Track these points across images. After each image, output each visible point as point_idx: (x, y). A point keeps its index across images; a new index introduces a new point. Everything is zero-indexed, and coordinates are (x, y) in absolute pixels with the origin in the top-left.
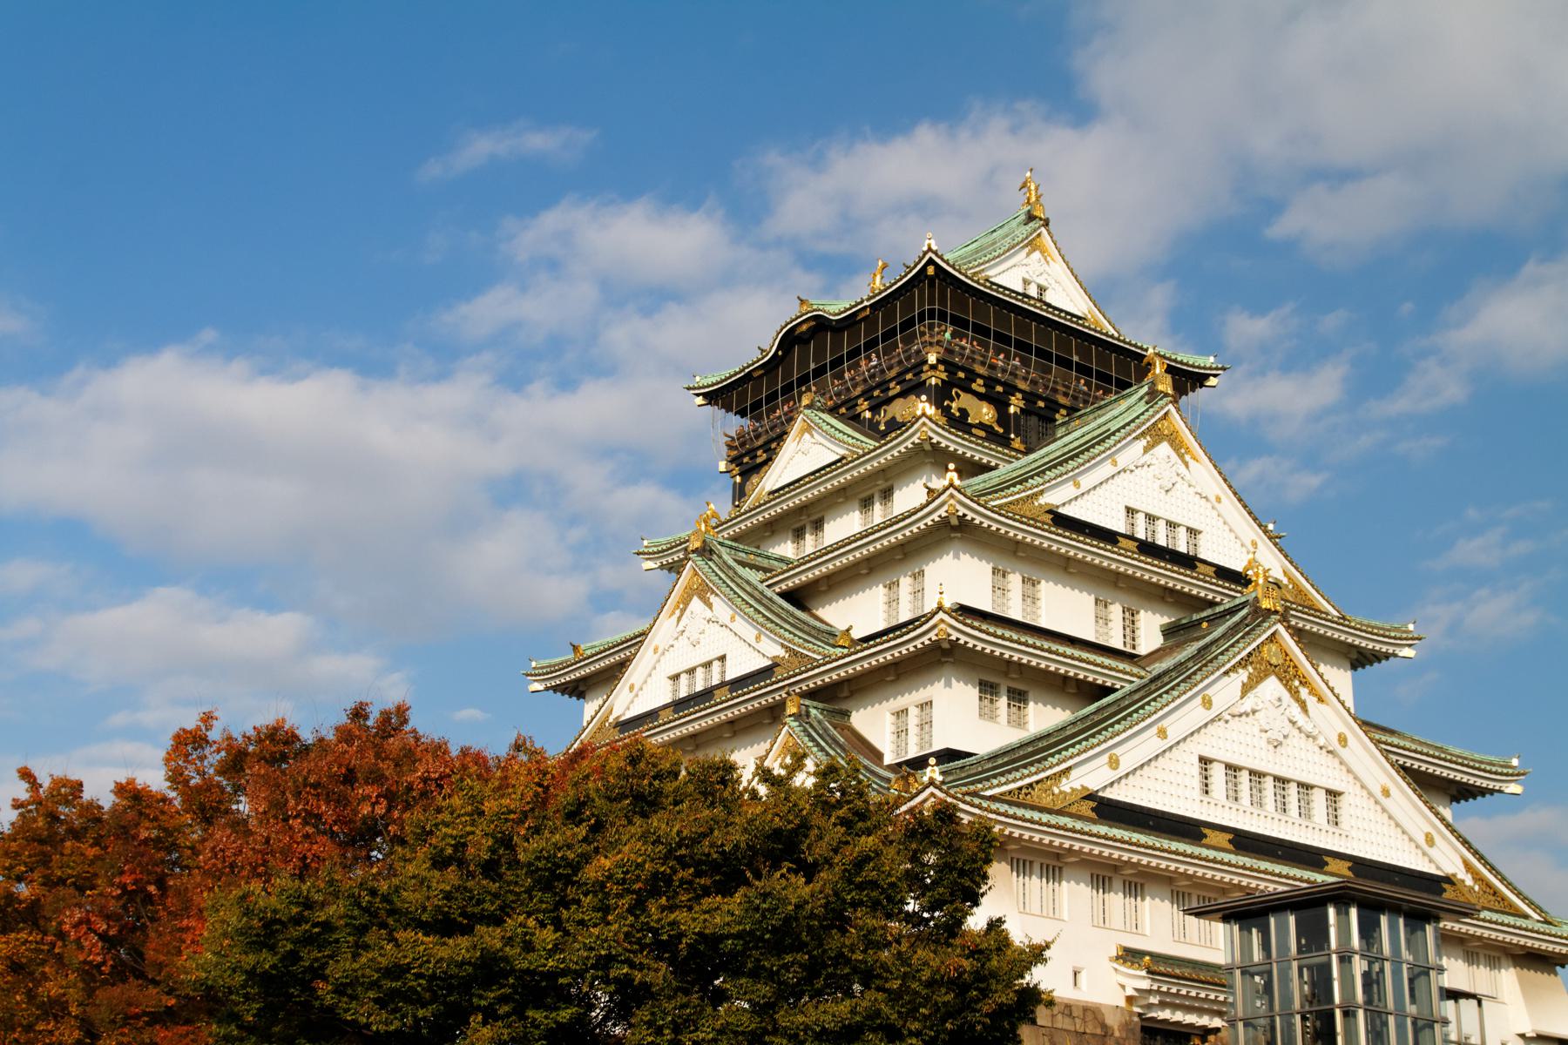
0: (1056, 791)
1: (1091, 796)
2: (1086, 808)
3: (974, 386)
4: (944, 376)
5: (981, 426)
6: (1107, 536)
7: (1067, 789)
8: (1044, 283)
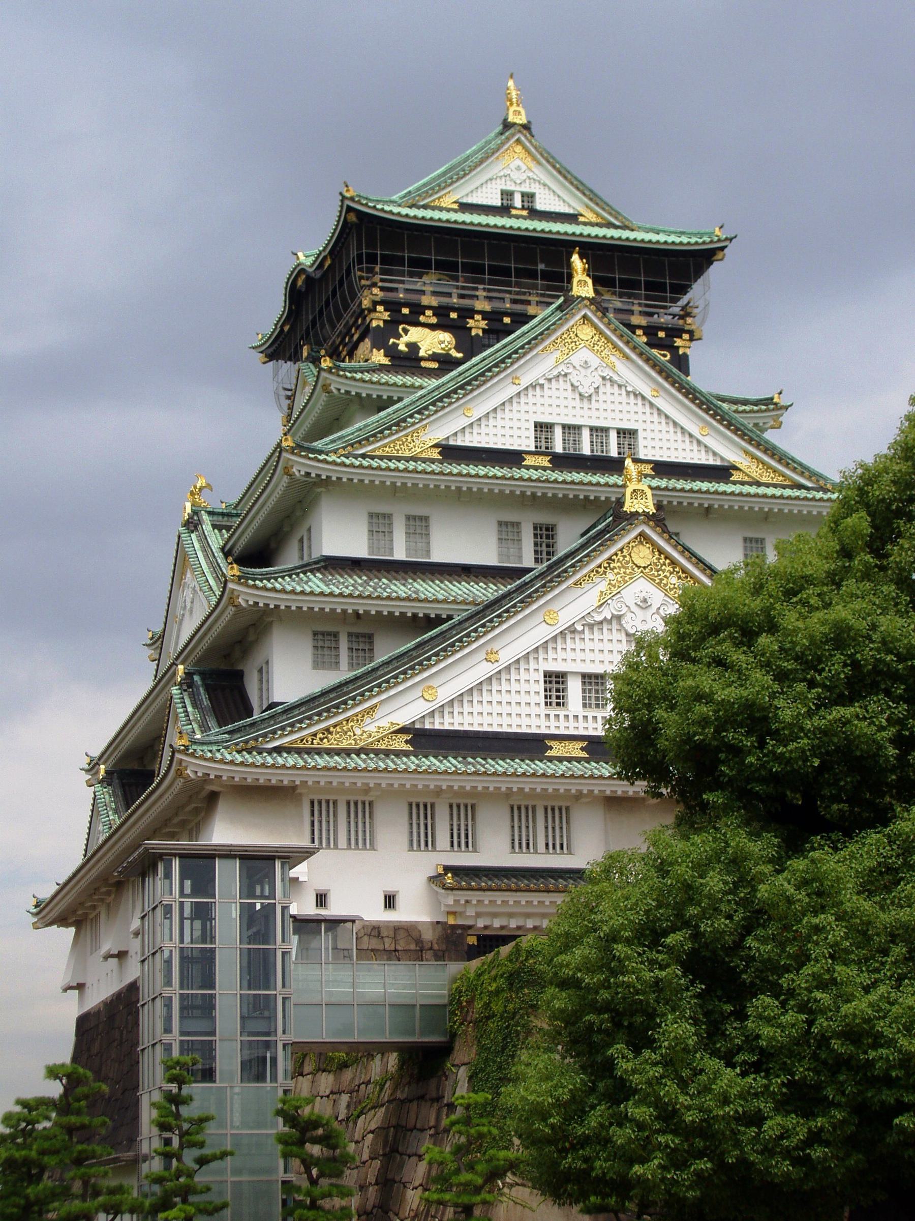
0: (358, 732)
1: (403, 730)
2: (400, 743)
3: (422, 319)
4: (386, 316)
5: (434, 357)
6: (512, 458)
7: (372, 728)
8: (526, 188)
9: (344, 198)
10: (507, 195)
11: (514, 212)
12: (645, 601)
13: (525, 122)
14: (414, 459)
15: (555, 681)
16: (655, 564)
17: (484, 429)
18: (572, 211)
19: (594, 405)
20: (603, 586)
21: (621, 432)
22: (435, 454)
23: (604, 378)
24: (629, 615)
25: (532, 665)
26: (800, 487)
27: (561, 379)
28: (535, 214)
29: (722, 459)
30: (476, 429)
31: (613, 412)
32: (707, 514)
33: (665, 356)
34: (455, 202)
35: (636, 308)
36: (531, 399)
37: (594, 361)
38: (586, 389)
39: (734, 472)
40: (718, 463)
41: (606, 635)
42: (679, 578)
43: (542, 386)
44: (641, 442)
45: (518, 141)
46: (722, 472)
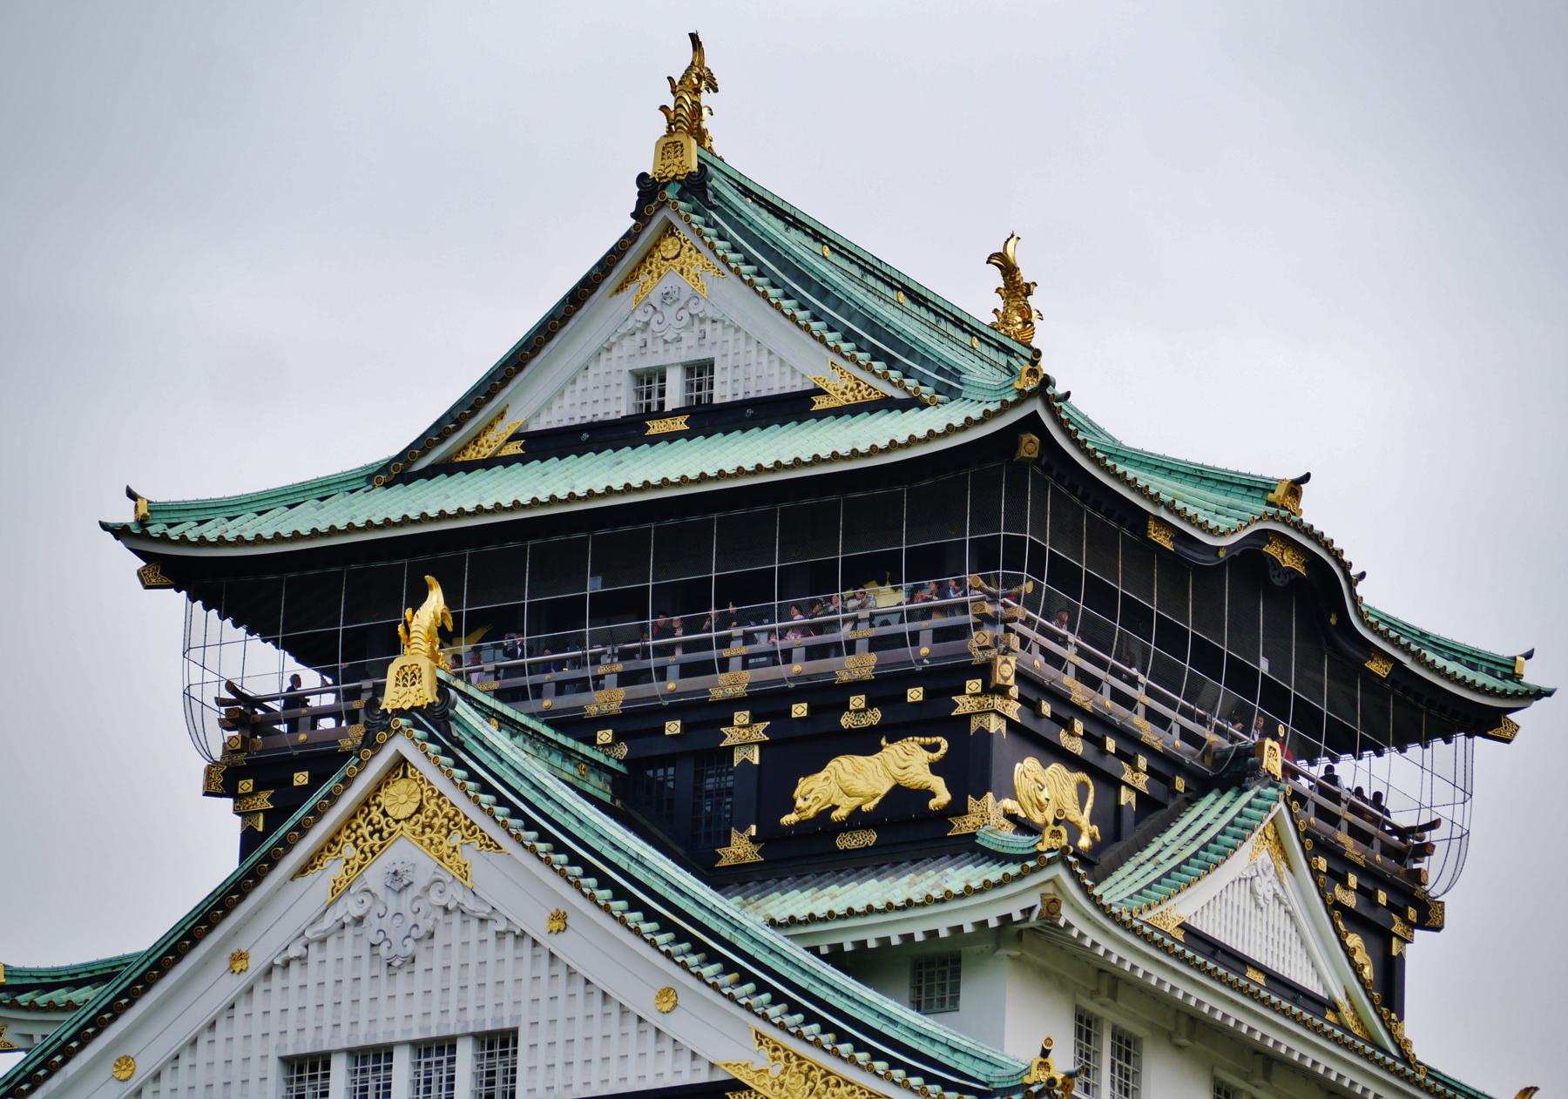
8: (691, 352)
9: (120, 532)
10: (649, 380)
11: (656, 427)
18: (799, 386)
19: (419, 982)
23: (446, 909)
27: (349, 932)
28: (708, 418)
29: (712, 1065)
33: (934, 748)
34: (514, 438)
36: (276, 1003)
38: (398, 949)
40: (703, 1077)
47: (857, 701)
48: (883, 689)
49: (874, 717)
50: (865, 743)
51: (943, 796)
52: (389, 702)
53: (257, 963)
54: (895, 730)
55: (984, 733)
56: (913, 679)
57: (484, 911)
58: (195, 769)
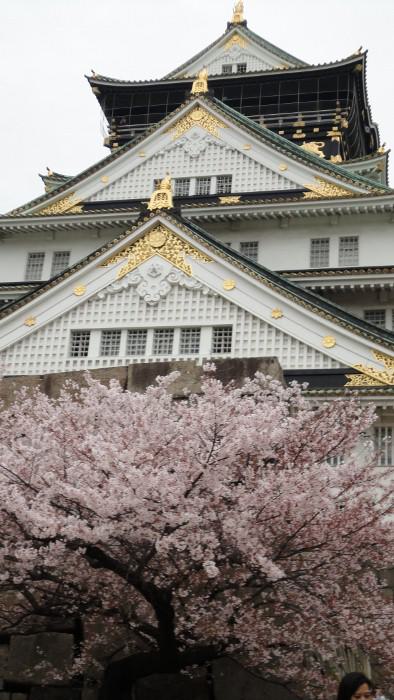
8: (240, 61)
9: (89, 79)
10: (227, 68)
12: (154, 271)
13: (242, 20)
14: (64, 214)
15: (80, 338)
16: (169, 245)
17: (116, 190)
19: (199, 164)
20: (125, 265)
21: (219, 177)
22: (79, 209)
23: (210, 144)
24: (144, 283)
25: (62, 326)
26: (362, 196)
27: (178, 149)
30: (110, 190)
31: (213, 166)
32: (281, 223)
33: (320, 145)
35: (300, 116)
37: (202, 133)
39: (306, 193)
41: (123, 300)
42: (187, 252)
43: (163, 156)
44: (233, 184)
45: (236, 33)
46: (297, 194)
47: (298, 131)
48: (307, 129)
49: (304, 135)
50: (300, 141)
51: (322, 155)
52: (193, 91)
53: (148, 156)
54: (308, 140)
55: (335, 141)
56: (316, 126)
57: (221, 144)
58: (102, 143)
